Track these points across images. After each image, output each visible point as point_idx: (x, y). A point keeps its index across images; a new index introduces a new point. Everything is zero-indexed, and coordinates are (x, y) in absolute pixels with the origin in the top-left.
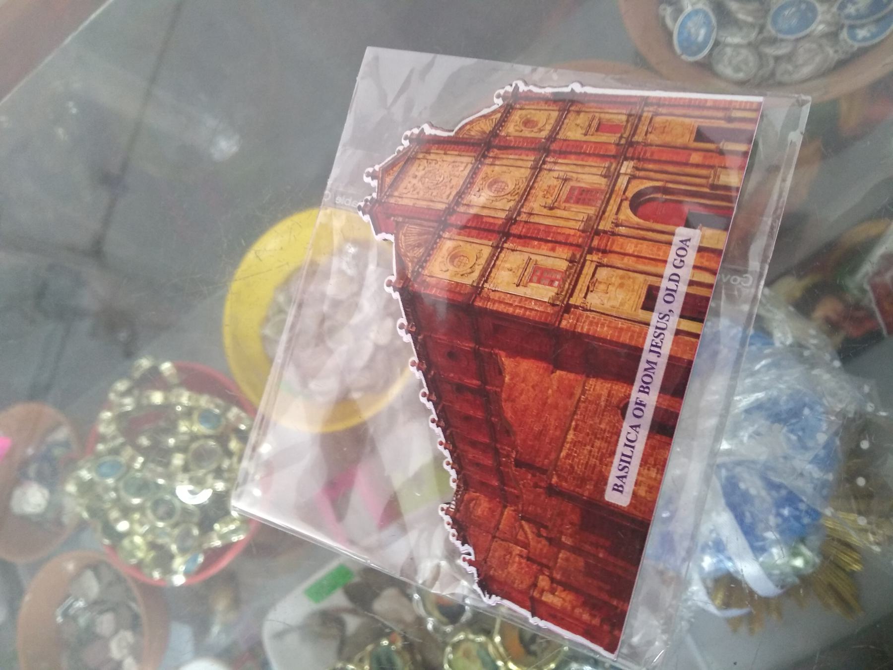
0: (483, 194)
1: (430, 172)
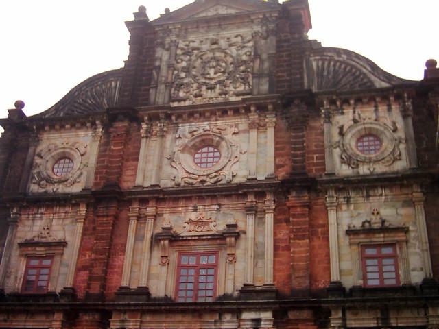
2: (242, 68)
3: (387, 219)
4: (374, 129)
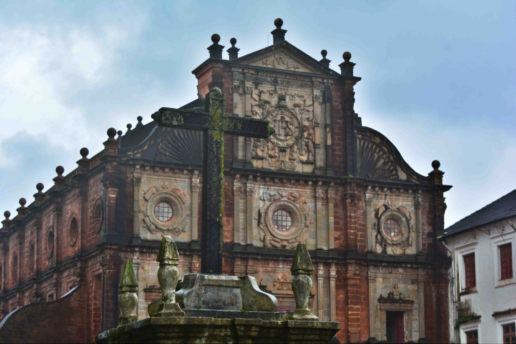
0: (268, 203)
1: (294, 116)
2: (306, 134)
4: (397, 215)
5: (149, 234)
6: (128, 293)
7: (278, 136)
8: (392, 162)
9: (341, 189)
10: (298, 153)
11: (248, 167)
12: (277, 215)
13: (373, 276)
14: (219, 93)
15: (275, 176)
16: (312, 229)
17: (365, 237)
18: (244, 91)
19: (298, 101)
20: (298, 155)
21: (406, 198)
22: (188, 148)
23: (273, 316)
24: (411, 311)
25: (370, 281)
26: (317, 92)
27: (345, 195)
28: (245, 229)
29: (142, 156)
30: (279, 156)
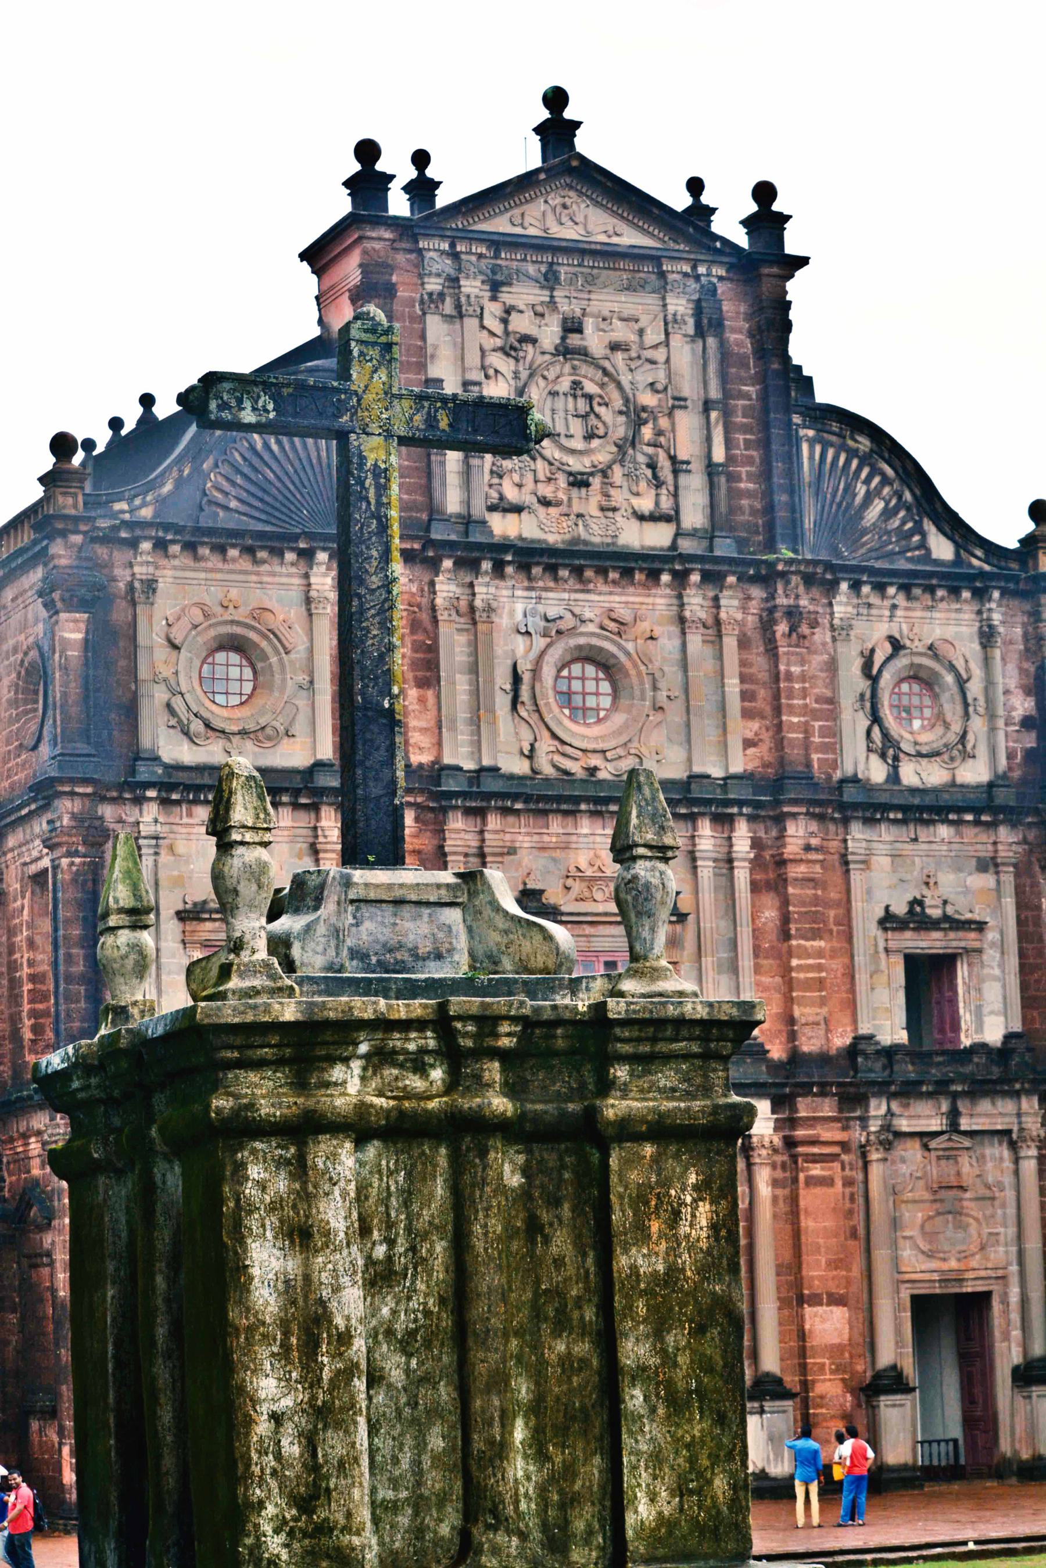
0: (540, 643)
2: (647, 432)
3: (951, 898)
5: (186, 747)
6: (126, 931)
7: (563, 441)
8: (908, 509)
9: (757, 593)
10: (625, 488)
11: (476, 537)
12: (570, 678)
13: (863, 851)
14: (379, 324)
15: (561, 561)
16: (675, 714)
17: (834, 736)
18: (458, 306)
19: (621, 332)
20: (628, 496)
21: (953, 615)
22: (294, 483)
23: (561, 987)
24: (979, 951)
25: (852, 866)
26: (679, 305)
27: (771, 611)
28: (476, 721)
29: (156, 514)
30: (570, 499)
